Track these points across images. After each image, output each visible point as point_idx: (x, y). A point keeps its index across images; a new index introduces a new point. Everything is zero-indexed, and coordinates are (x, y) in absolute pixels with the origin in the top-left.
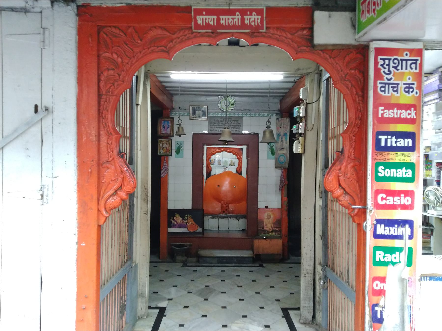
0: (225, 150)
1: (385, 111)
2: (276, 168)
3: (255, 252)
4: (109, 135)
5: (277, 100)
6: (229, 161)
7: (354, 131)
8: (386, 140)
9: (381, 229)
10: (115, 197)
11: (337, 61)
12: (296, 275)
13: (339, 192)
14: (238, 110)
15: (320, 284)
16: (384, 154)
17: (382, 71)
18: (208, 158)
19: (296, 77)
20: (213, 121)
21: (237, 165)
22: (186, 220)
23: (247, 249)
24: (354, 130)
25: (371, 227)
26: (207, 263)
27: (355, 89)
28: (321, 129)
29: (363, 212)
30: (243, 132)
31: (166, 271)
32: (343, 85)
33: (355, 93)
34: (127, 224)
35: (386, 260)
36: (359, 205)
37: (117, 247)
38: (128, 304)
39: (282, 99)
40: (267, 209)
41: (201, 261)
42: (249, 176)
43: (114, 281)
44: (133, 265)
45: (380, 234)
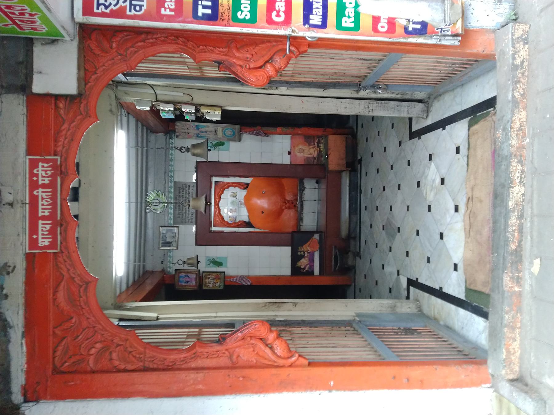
0: (217, 204)
1: (166, 6)
2: (240, 141)
3: (344, 168)
4: (196, 357)
5: (153, 137)
6: (231, 199)
7: (193, 46)
8: (204, 7)
9: (316, 19)
10: (275, 346)
11: (101, 64)
12: (371, 119)
13: (269, 69)
14: (165, 188)
15: (381, 94)
16: (221, 11)
17: (114, 8)
18: (228, 225)
19: (121, 114)
20: (180, 219)
21: (237, 189)
22: (304, 253)
23: (340, 178)
24: (190, 47)
25: (313, 31)
26: (356, 227)
27: (137, 42)
28: (190, 84)
29: (295, 40)
30: (194, 181)
31: (365, 278)
32: (132, 59)
33: (142, 43)
34: (308, 328)
35: (353, 14)
36: (286, 44)
37: (336, 341)
38: (403, 325)
39: (151, 130)
40: (292, 153)
41: (354, 235)
42: (250, 175)
43: (376, 343)
44: (357, 319)
45: (321, 20)
